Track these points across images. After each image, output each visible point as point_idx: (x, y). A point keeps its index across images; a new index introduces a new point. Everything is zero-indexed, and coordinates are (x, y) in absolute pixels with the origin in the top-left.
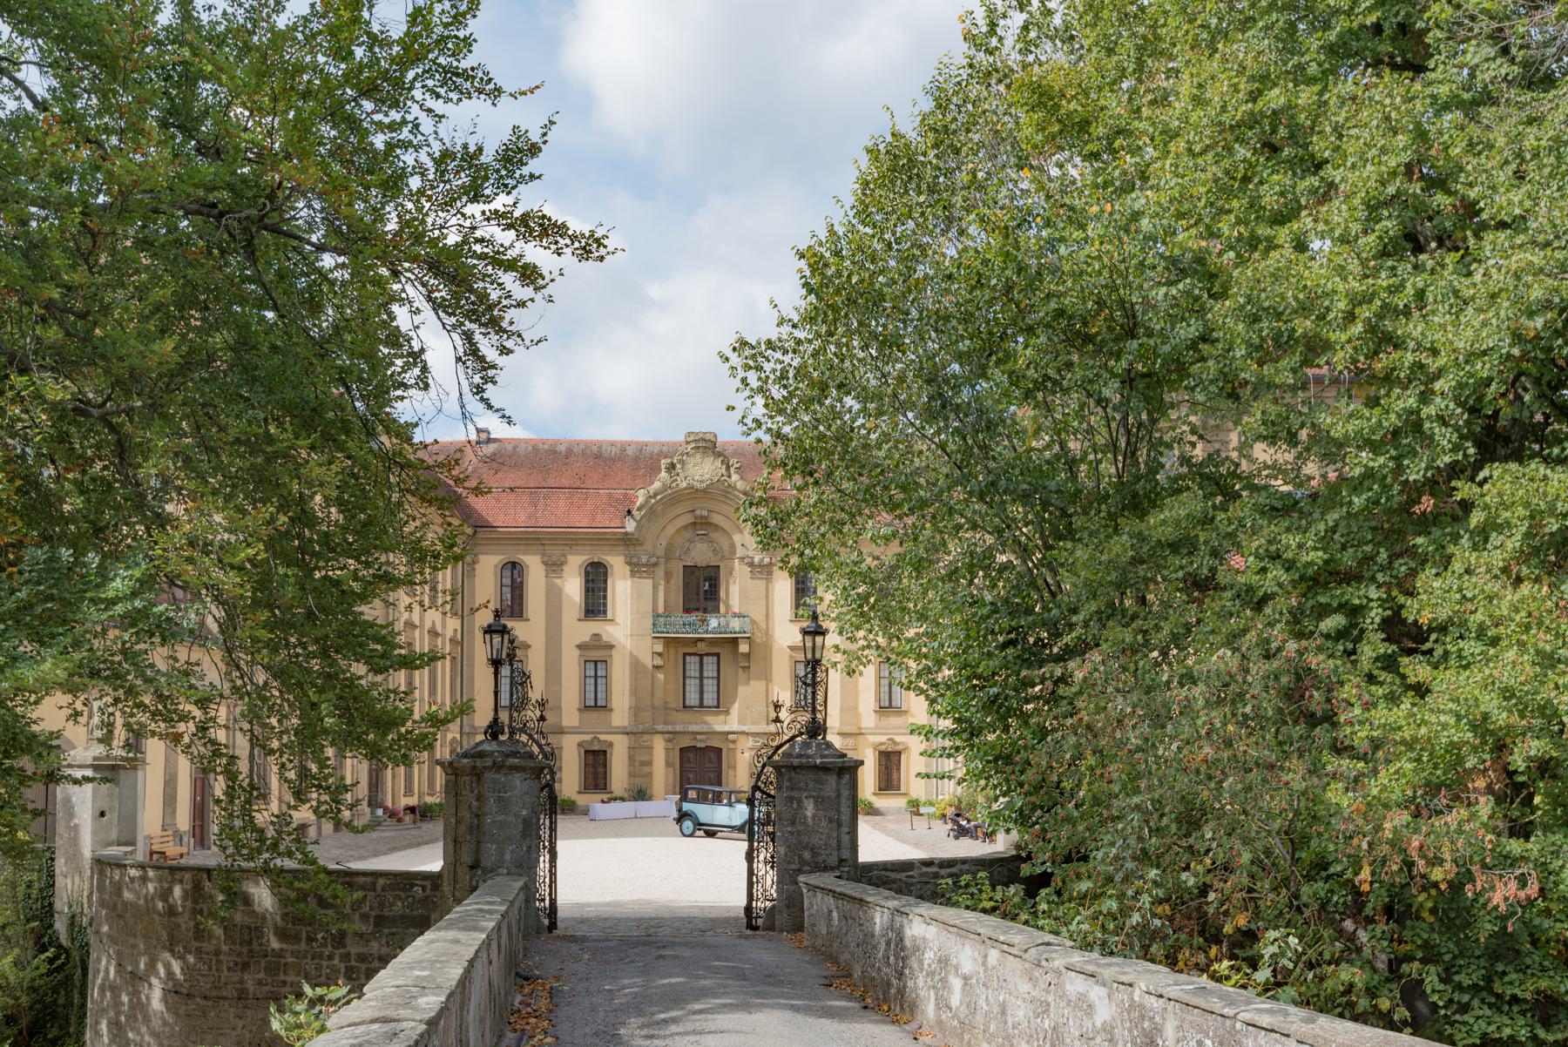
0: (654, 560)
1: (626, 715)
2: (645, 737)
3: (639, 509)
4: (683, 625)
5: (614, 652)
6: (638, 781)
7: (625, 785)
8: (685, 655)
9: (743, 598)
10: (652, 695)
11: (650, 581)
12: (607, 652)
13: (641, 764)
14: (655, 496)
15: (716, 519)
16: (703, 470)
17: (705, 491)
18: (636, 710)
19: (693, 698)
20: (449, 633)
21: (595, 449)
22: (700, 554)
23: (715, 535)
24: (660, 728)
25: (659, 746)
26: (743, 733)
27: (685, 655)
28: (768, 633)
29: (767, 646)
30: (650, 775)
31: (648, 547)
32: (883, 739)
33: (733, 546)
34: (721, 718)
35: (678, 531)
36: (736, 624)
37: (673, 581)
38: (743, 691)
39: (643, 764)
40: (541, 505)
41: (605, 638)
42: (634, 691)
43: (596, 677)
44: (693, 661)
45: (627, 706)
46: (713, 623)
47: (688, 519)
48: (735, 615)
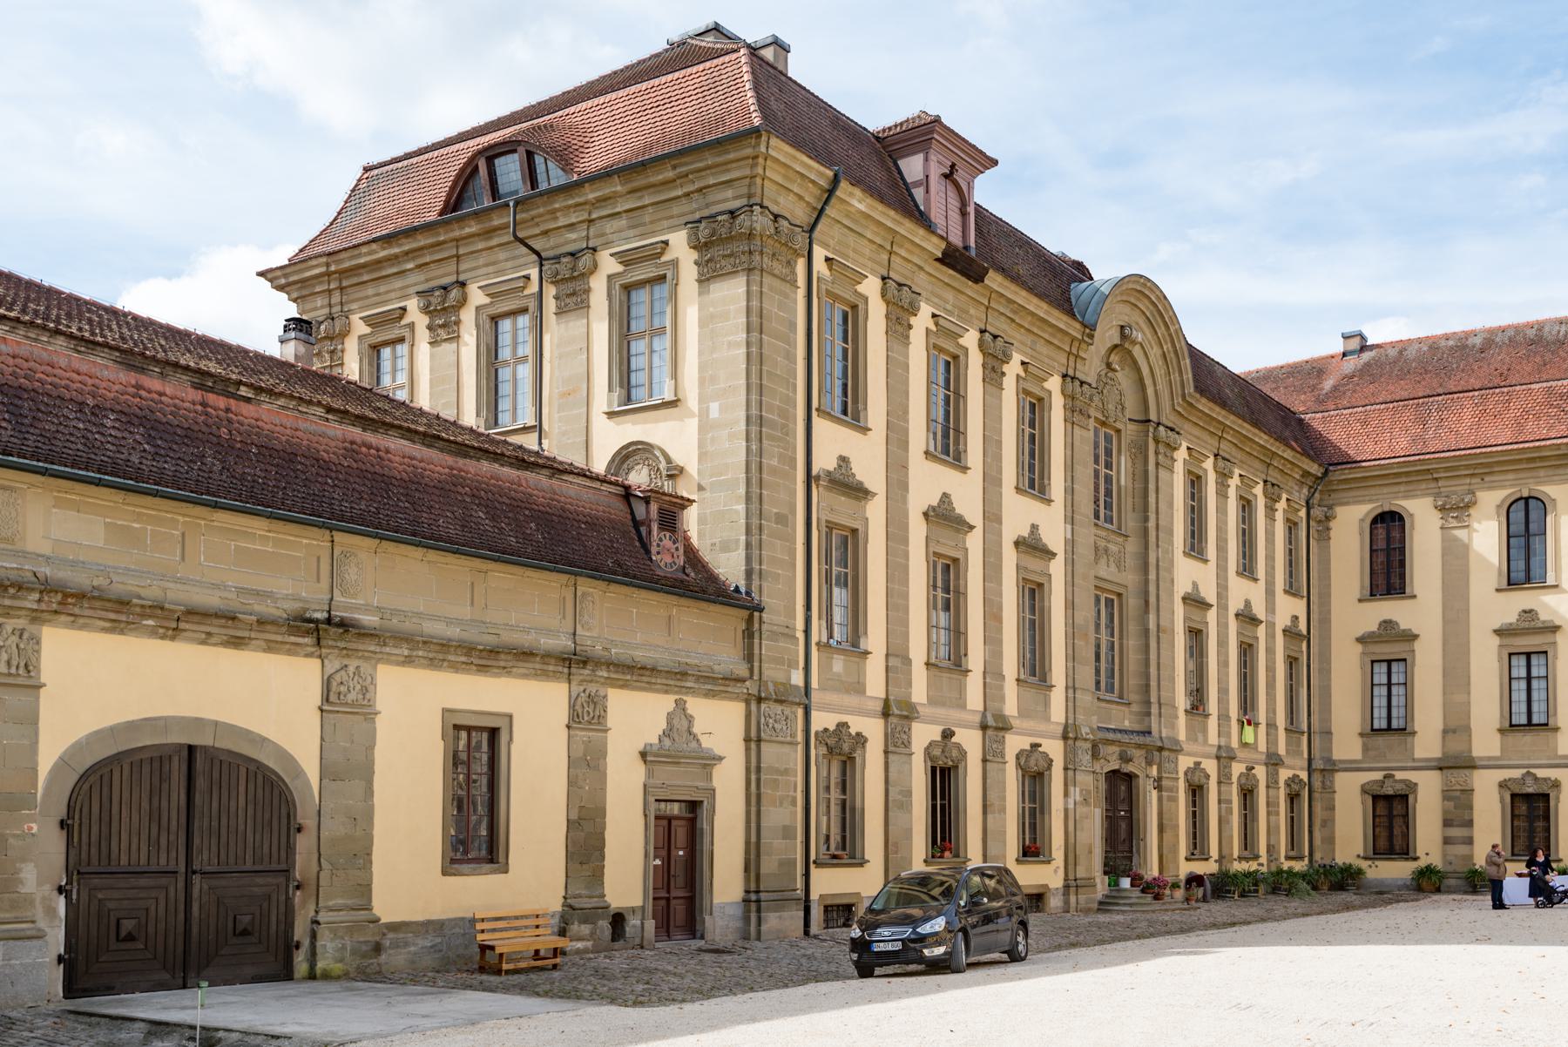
20: (1282, 621)
21: (1531, 333)
40: (1433, 422)
43: (1529, 679)
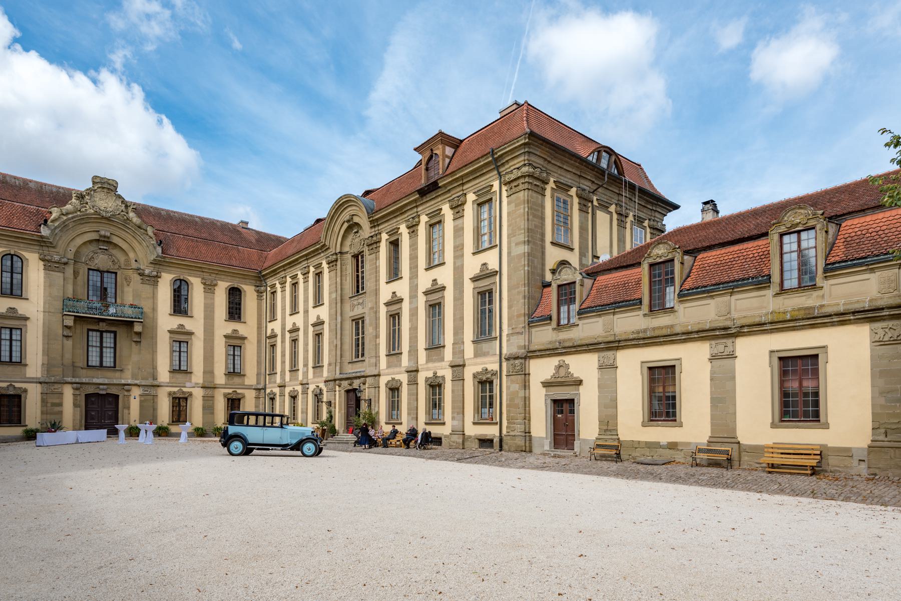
0: (65, 260)
1: (39, 370)
2: (56, 386)
3: (53, 221)
4: (90, 306)
5: (28, 323)
6: (52, 418)
7: (39, 420)
8: (89, 330)
9: (136, 295)
10: (62, 356)
11: (61, 275)
12: (23, 323)
13: (51, 404)
14: (67, 214)
15: (115, 240)
16: (105, 204)
17: (108, 219)
18: (48, 366)
19: (94, 360)
22: (102, 261)
23: (115, 252)
24: (69, 379)
25: (68, 393)
26: (136, 385)
27: (89, 330)
28: (154, 320)
29: (154, 328)
30: (61, 413)
31: (61, 248)
32: (230, 391)
33: (128, 261)
34: (118, 374)
35: (85, 243)
36: (129, 311)
37: (79, 278)
38: (135, 358)
39: (54, 405)
41: (20, 312)
42: (47, 352)
44: (94, 338)
45: (40, 363)
46: (112, 310)
47: (94, 236)
48: (131, 306)
